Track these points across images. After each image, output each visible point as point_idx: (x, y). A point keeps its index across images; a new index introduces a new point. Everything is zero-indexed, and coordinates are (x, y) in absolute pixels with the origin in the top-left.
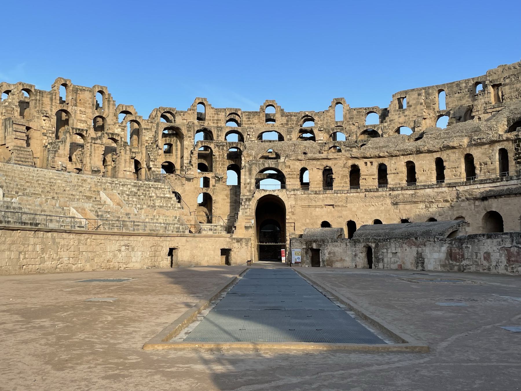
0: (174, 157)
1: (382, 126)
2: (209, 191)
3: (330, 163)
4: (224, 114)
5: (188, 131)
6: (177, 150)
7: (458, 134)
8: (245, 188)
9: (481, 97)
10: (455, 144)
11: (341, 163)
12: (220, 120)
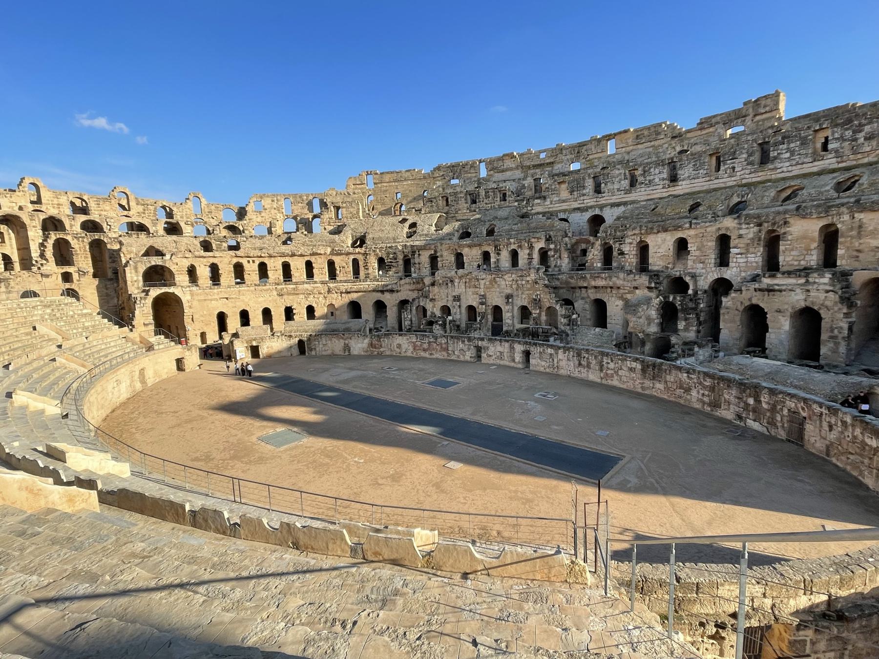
0: (8, 247)
3: (215, 261)
4: (65, 198)
6: (10, 239)
10: (322, 252)
11: (226, 260)
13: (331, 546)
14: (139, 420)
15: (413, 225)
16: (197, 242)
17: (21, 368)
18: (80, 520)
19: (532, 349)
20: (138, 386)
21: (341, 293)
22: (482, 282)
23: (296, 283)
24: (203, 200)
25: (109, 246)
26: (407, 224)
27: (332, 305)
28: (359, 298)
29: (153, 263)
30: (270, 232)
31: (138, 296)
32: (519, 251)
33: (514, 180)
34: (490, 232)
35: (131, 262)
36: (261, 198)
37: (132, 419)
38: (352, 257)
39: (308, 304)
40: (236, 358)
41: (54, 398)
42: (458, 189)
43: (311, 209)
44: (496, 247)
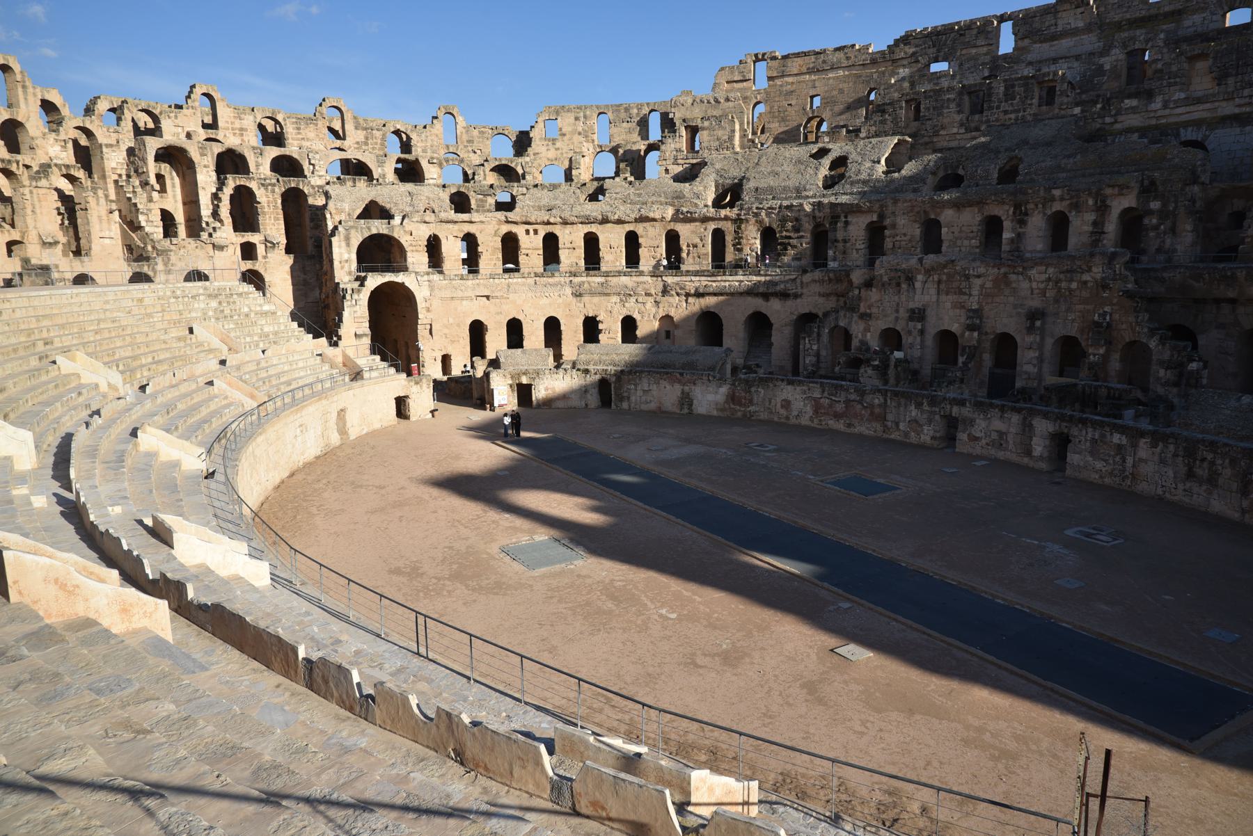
1: (520, 160)
2: (258, 266)
4: (251, 118)
5: (202, 155)
6: (173, 186)
7: (654, 198)
8: (342, 268)
9: (670, 140)
10: (657, 216)
12: (246, 130)
13: (517, 771)
14: (326, 495)
15: (840, 162)
16: (445, 196)
17: (161, 392)
18: (120, 646)
19: (1074, 431)
20: (335, 439)
21: (688, 295)
22: (978, 282)
23: (607, 274)
24: (460, 119)
25: (311, 201)
26: (827, 161)
27: (667, 318)
28: (717, 305)
29: (374, 231)
30: (568, 177)
31: (349, 287)
32: (1072, 216)
33: (1077, 57)
34: (1008, 175)
35: (340, 228)
36: (557, 113)
37: (315, 490)
38: (712, 226)
39: (625, 312)
40: (492, 405)
41: (200, 444)
42: (945, 83)
43: (644, 134)
44: (1017, 207)
